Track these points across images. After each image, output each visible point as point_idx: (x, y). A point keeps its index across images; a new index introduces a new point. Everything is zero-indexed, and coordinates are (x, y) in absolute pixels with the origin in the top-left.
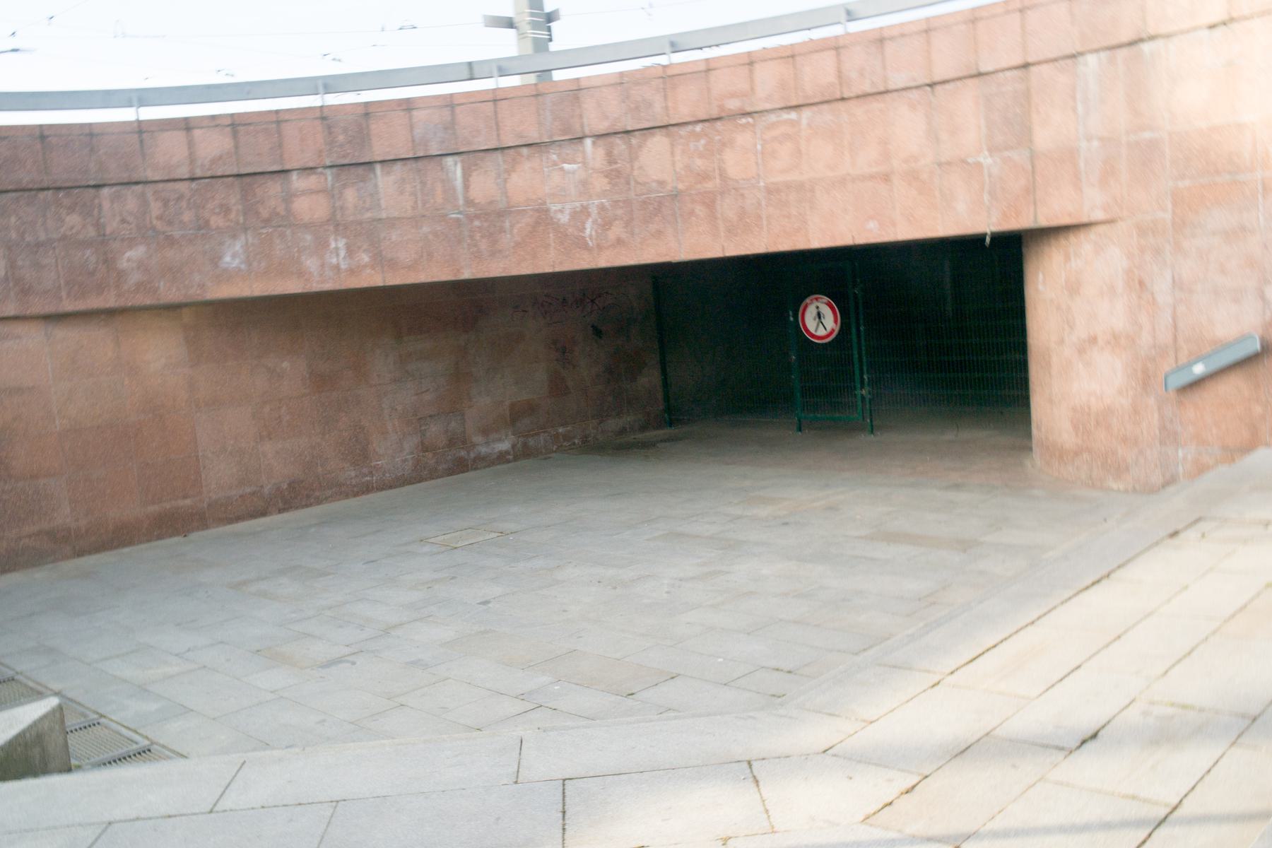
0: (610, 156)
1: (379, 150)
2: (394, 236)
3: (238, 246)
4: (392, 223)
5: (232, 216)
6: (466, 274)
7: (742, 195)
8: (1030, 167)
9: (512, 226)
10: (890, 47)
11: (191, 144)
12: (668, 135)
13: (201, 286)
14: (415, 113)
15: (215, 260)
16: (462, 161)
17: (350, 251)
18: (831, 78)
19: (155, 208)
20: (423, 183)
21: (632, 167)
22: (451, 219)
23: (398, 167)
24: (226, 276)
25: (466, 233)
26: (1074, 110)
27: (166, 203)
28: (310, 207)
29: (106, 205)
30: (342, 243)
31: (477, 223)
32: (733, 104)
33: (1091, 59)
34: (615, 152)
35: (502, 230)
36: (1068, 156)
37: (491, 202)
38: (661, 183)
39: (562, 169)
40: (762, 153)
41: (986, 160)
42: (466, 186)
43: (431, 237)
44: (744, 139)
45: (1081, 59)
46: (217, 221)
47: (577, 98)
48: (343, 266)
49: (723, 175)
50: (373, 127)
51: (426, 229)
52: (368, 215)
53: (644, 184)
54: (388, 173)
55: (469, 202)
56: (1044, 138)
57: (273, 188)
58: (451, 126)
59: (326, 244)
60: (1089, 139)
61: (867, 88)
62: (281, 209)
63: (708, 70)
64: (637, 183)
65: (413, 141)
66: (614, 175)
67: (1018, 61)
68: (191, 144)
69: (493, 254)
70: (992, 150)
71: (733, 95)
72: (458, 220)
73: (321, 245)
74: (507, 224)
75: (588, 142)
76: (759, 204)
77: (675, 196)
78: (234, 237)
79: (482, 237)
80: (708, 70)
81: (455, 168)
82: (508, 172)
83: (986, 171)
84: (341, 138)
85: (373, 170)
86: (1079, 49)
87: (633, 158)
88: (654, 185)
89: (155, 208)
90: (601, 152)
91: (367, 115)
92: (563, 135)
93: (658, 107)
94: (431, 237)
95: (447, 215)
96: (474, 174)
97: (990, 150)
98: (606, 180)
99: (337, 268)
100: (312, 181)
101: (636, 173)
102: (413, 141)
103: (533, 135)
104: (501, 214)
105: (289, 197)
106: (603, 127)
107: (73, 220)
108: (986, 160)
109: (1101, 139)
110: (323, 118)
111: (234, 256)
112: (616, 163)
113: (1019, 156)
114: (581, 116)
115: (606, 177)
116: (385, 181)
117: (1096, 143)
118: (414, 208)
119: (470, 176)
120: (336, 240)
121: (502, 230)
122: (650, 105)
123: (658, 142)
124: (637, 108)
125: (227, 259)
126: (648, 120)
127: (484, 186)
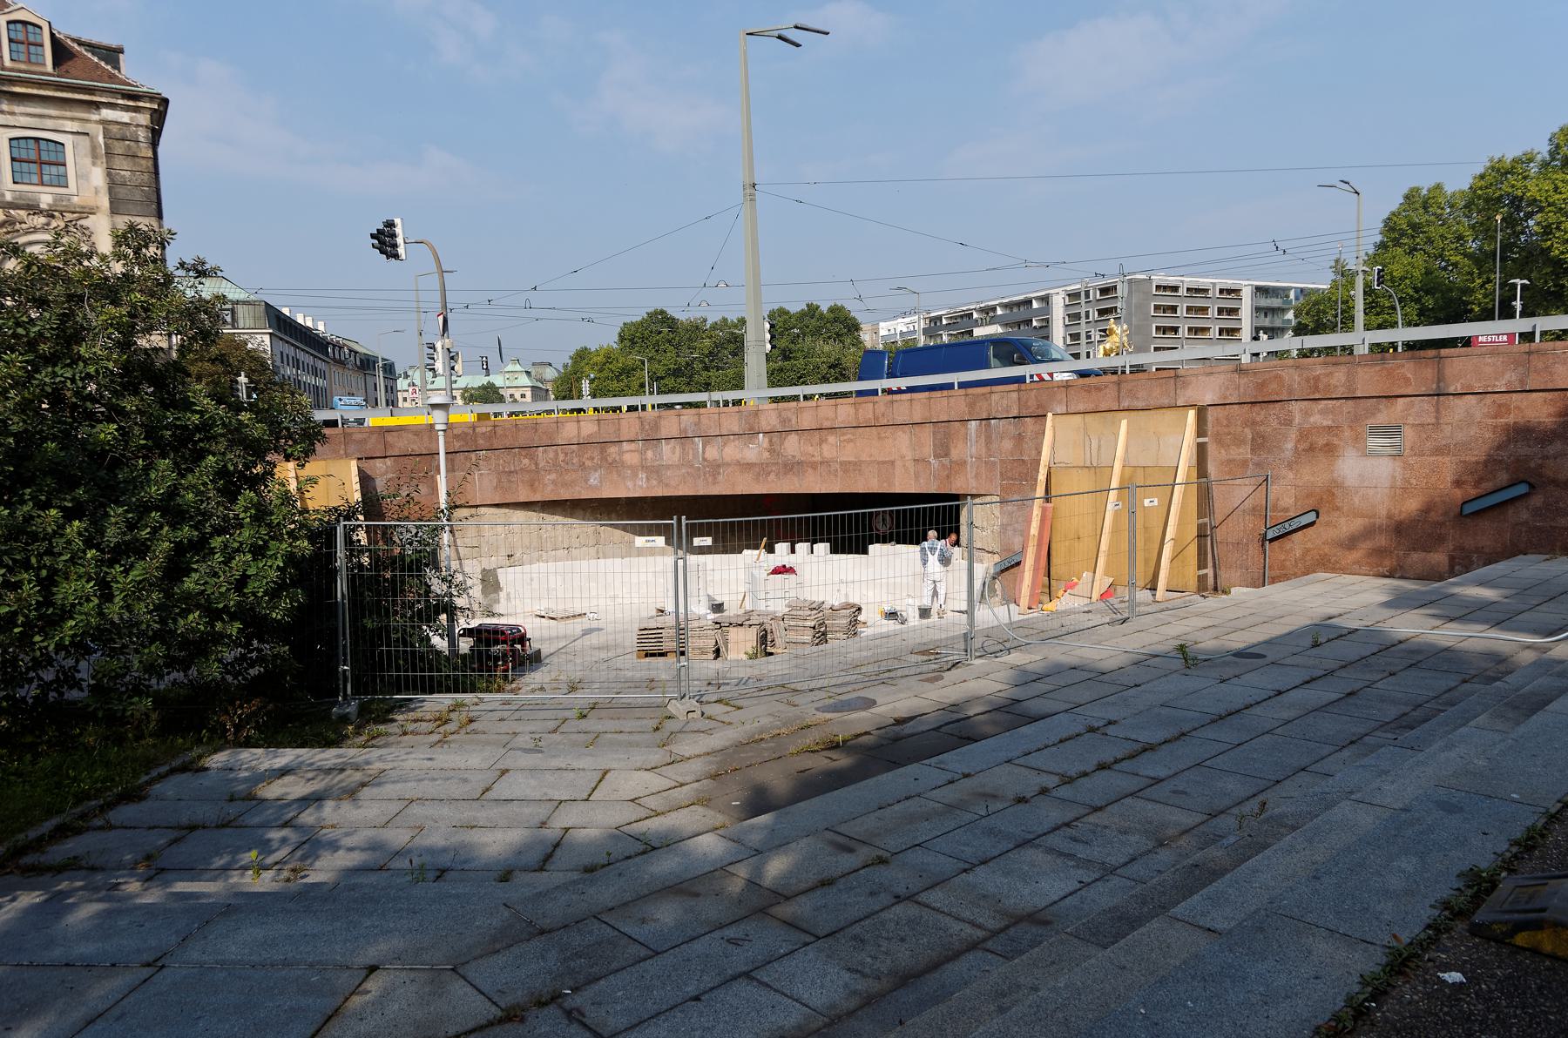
0: (770, 441)
2: (669, 473)
3: (597, 475)
4: (668, 467)
6: (701, 493)
10: (895, 405)
11: (579, 428)
13: (580, 492)
15: (586, 481)
18: (871, 416)
19: (561, 457)
20: (684, 449)
24: (591, 487)
27: (566, 454)
28: (631, 458)
29: (540, 455)
30: (644, 476)
32: (827, 424)
35: (719, 473)
36: (962, 463)
41: (932, 460)
42: (704, 453)
44: (832, 439)
46: (588, 463)
48: (645, 486)
54: (668, 444)
55: (704, 459)
56: (955, 454)
57: (613, 449)
58: (698, 424)
59: (637, 476)
61: (885, 422)
62: (617, 458)
66: (771, 451)
68: (579, 428)
69: (714, 484)
70: (936, 456)
71: (827, 419)
73: (635, 475)
77: (799, 463)
78: (596, 470)
81: (699, 442)
89: (561, 457)
90: (767, 440)
93: (794, 422)
99: (641, 487)
100: (633, 446)
103: (736, 429)
104: (719, 466)
105: (621, 453)
106: (767, 430)
107: (526, 461)
108: (932, 460)
113: (946, 461)
116: (666, 448)
121: (719, 473)
122: (790, 421)
123: (793, 438)
127: (712, 453)
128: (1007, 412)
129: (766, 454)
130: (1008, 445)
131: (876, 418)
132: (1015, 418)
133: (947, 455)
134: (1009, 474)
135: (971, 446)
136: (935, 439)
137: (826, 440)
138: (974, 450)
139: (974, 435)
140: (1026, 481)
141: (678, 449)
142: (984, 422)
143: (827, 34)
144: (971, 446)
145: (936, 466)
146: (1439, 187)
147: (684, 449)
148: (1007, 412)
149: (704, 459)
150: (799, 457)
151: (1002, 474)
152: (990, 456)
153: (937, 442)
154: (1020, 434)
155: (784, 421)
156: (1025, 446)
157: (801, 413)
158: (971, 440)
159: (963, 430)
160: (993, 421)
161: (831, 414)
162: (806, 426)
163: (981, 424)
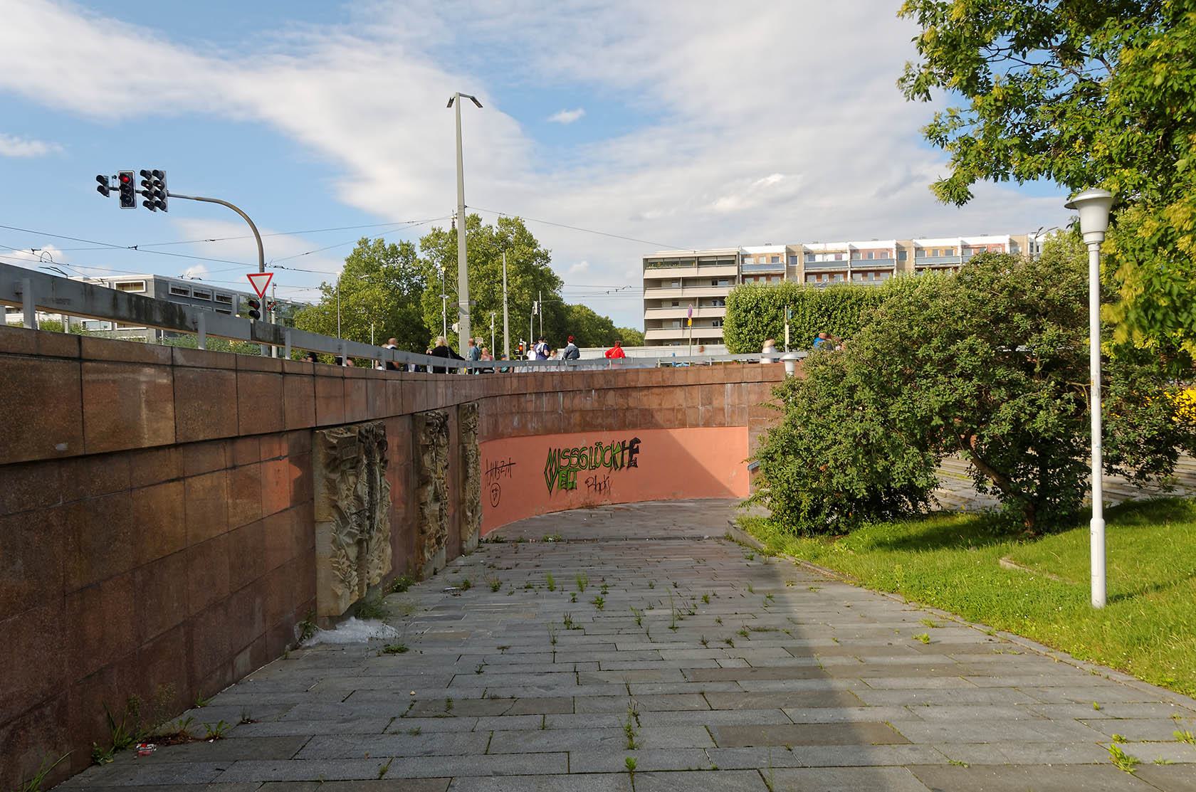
0: (598, 395)
28: (531, 407)
31: (566, 415)
32: (633, 384)
38: (612, 406)
56: (716, 403)
63: (626, 373)
80: (626, 373)
85: (542, 395)
87: (605, 394)
91: (543, 376)
93: (613, 383)
106: (598, 387)
113: (709, 407)
116: (545, 398)
122: (611, 381)
123: (612, 393)
127: (568, 403)
129: (596, 405)
131: (663, 380)
133: (710, 403)
135: (728, 398)
137: (631, 395)
138: (730, 400)
142: (737, 385)
143: (480, 106)
144: (728, 398)
145: (703, 410)
146: (381, 242)
150: (615, 407)
151: (749, 415)
152: (741, 404)
153: (704, 397)
154: (762, 391)
160: (743, 384)
162: (620, 385)
163: (734, 386)
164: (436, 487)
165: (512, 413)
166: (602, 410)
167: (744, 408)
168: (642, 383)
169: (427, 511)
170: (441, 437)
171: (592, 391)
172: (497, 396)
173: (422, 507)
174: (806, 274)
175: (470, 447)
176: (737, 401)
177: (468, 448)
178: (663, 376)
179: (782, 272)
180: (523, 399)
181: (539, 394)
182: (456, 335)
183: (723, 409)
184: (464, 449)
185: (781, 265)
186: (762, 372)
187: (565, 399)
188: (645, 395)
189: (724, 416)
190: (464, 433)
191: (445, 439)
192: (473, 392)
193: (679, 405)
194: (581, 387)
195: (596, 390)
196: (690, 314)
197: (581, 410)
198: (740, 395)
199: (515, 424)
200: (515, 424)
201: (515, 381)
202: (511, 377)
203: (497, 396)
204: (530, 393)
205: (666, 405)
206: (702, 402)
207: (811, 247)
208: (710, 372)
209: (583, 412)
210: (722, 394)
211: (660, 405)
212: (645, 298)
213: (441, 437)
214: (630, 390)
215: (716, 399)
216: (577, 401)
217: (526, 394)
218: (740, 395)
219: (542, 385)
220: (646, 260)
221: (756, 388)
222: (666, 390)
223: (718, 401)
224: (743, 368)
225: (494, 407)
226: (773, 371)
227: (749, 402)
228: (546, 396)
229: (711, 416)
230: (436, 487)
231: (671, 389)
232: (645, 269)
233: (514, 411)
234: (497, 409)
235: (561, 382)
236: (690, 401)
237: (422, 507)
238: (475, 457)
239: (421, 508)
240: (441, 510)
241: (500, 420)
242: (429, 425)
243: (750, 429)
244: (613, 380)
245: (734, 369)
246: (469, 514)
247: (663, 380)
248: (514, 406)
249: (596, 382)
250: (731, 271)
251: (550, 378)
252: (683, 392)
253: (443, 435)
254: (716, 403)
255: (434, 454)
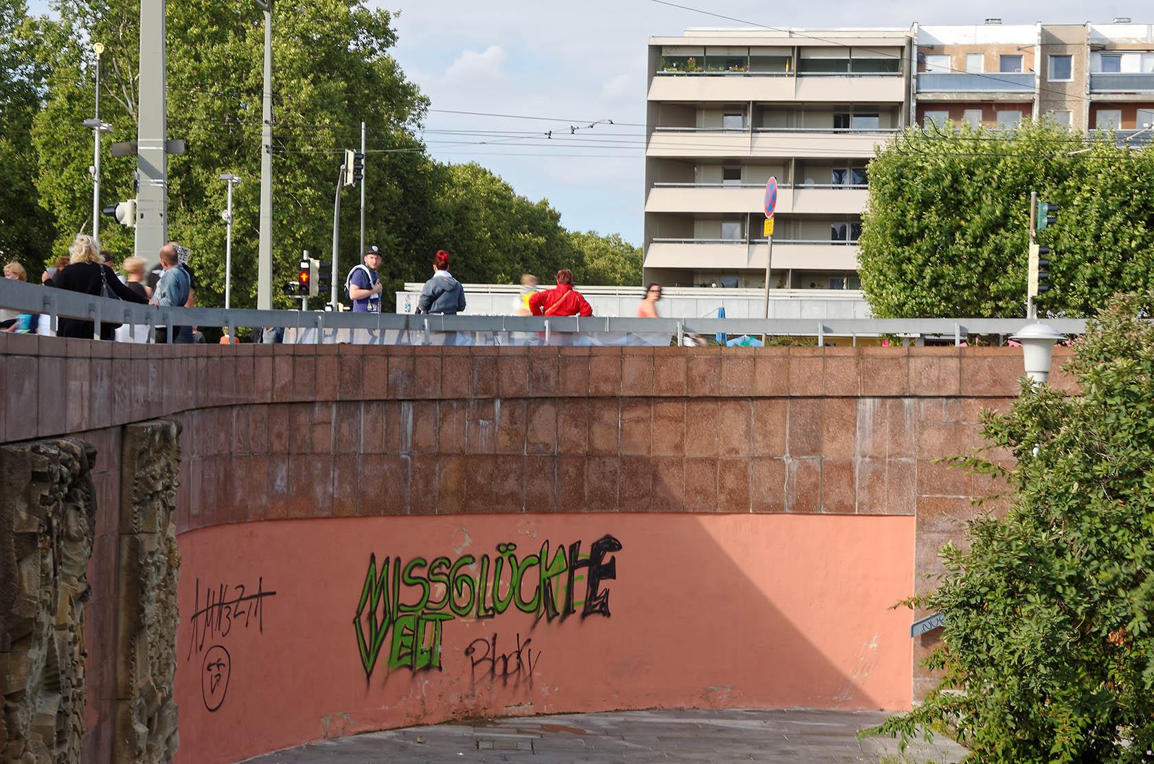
0: (512, 415)
1: (368, 392)
5: (283, 442)
7: (604, 463)
8: (820, 470)
9: (440, 470)
12: (554, 404)
14: (391, 359)
16: (414, 407)
17: (341, 483)
18: (682, 378)
21: (527, 428)
22: (402, 459)
23: (374, 406)
25: (410, 473)
26: (854, 433)
28: (324, 439)
31: (418, 465)
32: (606, 389)
33: (869, 401)
34: (516, 414)
37: (429, 447)
38: (546, 445)
39: (478, 423)
40: (622, 430)
42: (414, 431)
43: (388, 474)
45: (862, 400)
47: (496, 363)
49: (590, 441)
50: (366, 368)
51: (386, 467)
52: (353, 449)
53: (534, 444)
56: (831, 451)
58: (412, 375)
60: (864, 456)
61: (706, 391)
63: (590, 356)
64: (529, 442)
65: (388, 384)
67: (819, 393)
70: (794, 453)
72: (406, 460)
74: (437, 469)
75: (498, 404)
76: (616, 472)
79: (420, 478)
80: (590, 356)
81: (408, 411)
82: (442, 420)
83: (787, 466)
84: (347, 376)
85: (358, 408)
86: (863, 394)
87: (528, 421)
88: (541, 446)
90: (506, 412)
91: (363, 356)
92: (485, 393)
93: (552, 381)
94: (388, 474)
95: (399, 456)
96: (420, 420)
97: (791, 453)
98: (508, 437)
101: (529, 434)
102: (388, 384)
106: (510, 391)
109: (870, 457)
110: (339, 356)
111: (281, 480)
112: (516, 424)
114: (498, 380)
115: (508, 434)
116: (364, 418)
117: (867, 459)
118: (381, 446)
119: (418, 421)
120: (334, 470)
121: (434, 474)
122: (547, 378)
123: (546, 412)
124: (538, 379)
125: (279, 482)
126: (544, 391)
128: (939, 387)
129: (503, 439)
130: (934, 439)
131: (690, 381)
132: (948, 397)
133: (815, 450)
134: (937, 484)
136: (793, 423)
139: (869, 421)
140: (966, 493)
141: (381, 425)
142: (889, 402)
144: (863, 438)
145: (794, 468)
147: (387, 423)
148: (939, 387)
149: (415, 445)
151: (921, 483)
152: (900, 454)
154: (957, 422)
155: (537, 379)
156: (966, 440)
157: (565, 367)
158: (863, 428)
159: (848, 411)
160: (906, 401)
161: (613, 372)
162: (571, 389)
164: (51, 651)
165: (271, 454)
166: (519, 457)
167: (907, 466)
168: (632, 387)
169: (22, 718)
170: (72, 514)
171: (492, 401)
172: (232, 406)
173: (10, 704)
174: (1095, 107)
175: (151, 544)
176: (888, 447)
177: (148, 547)
178: (689, 369)
179: (1027, 98)
180: (303, 418)
181: (348, 405)
182: (127, 232)
183: (848, 467)
184: (136, 548)
185: (1026, 79)
186: (961, 369)
187: (420, 423)
188: (638, 421)
189: (852, 480)
190: (136, 504)
191: (84, 520)
192: (165, 392)
193: (730, 451)
194: (465, 390)
195: (506, 400)
196: (772, 201)
197: (462, 453)
198: (897, 431)
199: (280, 484)
200: (280, 484)
201: (284, 367)
202: (273, 357)
203: (232, 406)
204: (326, 403)
205: (693, 450)
206: (792, 443)
207: (1112, 33)
208: (818, 365)
209: (467, 459)
210: (849, 424)
211: (678, 447)
212: (653, 152)
213: (72, 514)
214: (599, 404)
215: (833, 439)
216: (450, 428)
217: (312, 403)
218: (897, 431)
219: (358, 379)
220: (656, 50)
221: (942, 413)
222: (697, 407)
223: (836, 445)
224: (909, 356)
225: (222, 435)
226: (991, 368)
227: (921, 450)
228: (367, 412)
229: (816, 486)
230: (51, 651)
231: (710, 406)
232: (654, 71)
233: (277, 446)
234: (230, 444)
235: (412, 375)
236: (759, 438)
237: (10, 704)
238: (164, 571)
239: (7, 709)
240: (62, 714)
241: (240, 472)
242: (39, 477)
243: (921, 525)
244: (553, 374)
245: (883, 359)
246: (141, 729)
247: (690, 381)
248: (279, 436)
249: (506, 380)
250: (889, 89)
251: (381, 361)
252: (742, 417)
253: (78, 509)
254: (831, 451)
255: (49, 560)
